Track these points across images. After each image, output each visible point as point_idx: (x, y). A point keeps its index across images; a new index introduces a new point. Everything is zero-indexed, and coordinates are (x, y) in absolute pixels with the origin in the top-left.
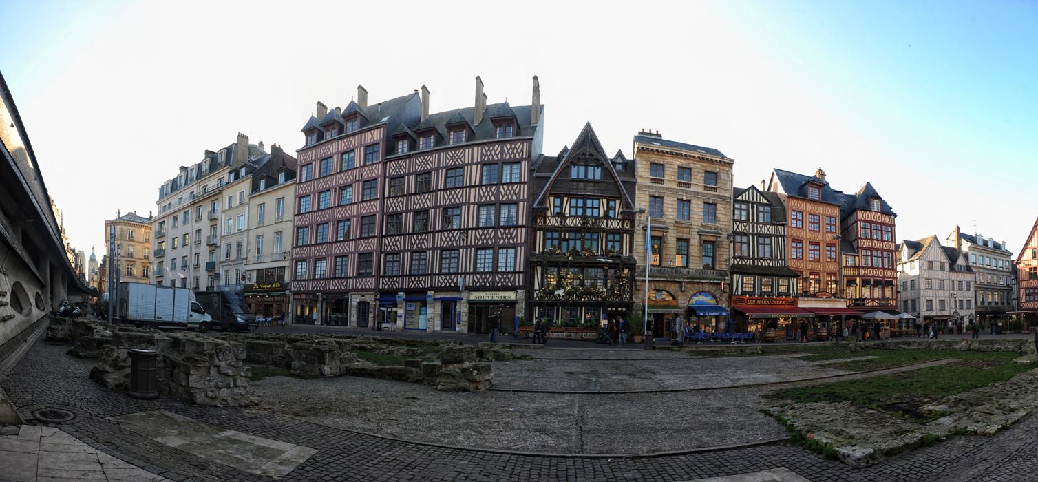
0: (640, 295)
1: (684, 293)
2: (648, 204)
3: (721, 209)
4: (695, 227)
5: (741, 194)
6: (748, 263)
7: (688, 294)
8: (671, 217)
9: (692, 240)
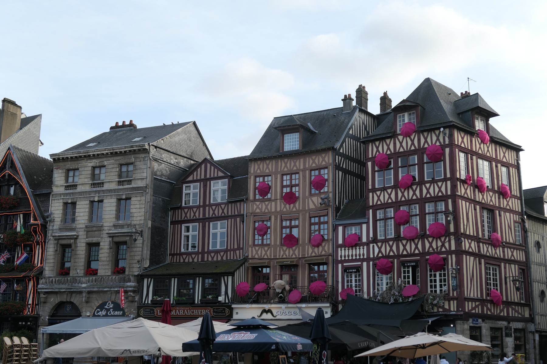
0: (46, 308)
3: (137, 202)
5: (192, 173)
6: (196, 260)
8: (83, 221)
9: (101, 244)
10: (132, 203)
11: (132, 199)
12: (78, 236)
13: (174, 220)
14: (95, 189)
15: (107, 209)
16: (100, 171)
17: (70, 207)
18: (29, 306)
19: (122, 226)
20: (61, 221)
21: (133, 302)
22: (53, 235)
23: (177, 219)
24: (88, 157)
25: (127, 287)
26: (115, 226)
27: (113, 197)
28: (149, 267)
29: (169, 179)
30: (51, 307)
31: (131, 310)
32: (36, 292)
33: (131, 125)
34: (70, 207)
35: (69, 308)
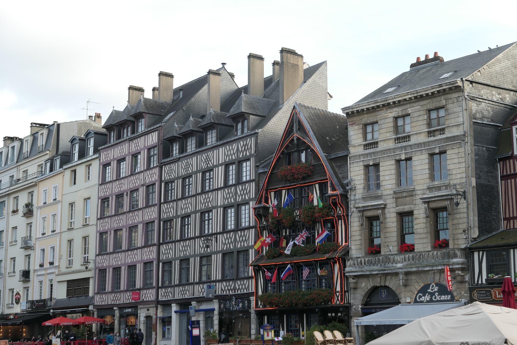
0: (358, 295)
1: (408, 289)
2: (363, 177)
3: (454, 156)
4: (418, 192)
7: (413, 288)
8: (390, 186)
9: (415, 212)
10: (448, 157)
11: (448, 152)
12: (385, 205)
13: (505, 173)
14: (400, 145)
15: (418, 168)
16: (404, 122)
17: (372, 169)
18: (338, 294)
19: (439, 188)
20: (364, 188)
21: (462, 282)
22: (357, 206)
23: (509, 173)
24: (388, 106)
25: (454, 264)
26: (430, 189)
27: (424, 152)
28: (479, 237)
29: (492, 121)
30: (363, 293)
31: (461, 293)
32: (344, 277)
33: (436, 58)
34: (372, 169)
35: (384, 294)
